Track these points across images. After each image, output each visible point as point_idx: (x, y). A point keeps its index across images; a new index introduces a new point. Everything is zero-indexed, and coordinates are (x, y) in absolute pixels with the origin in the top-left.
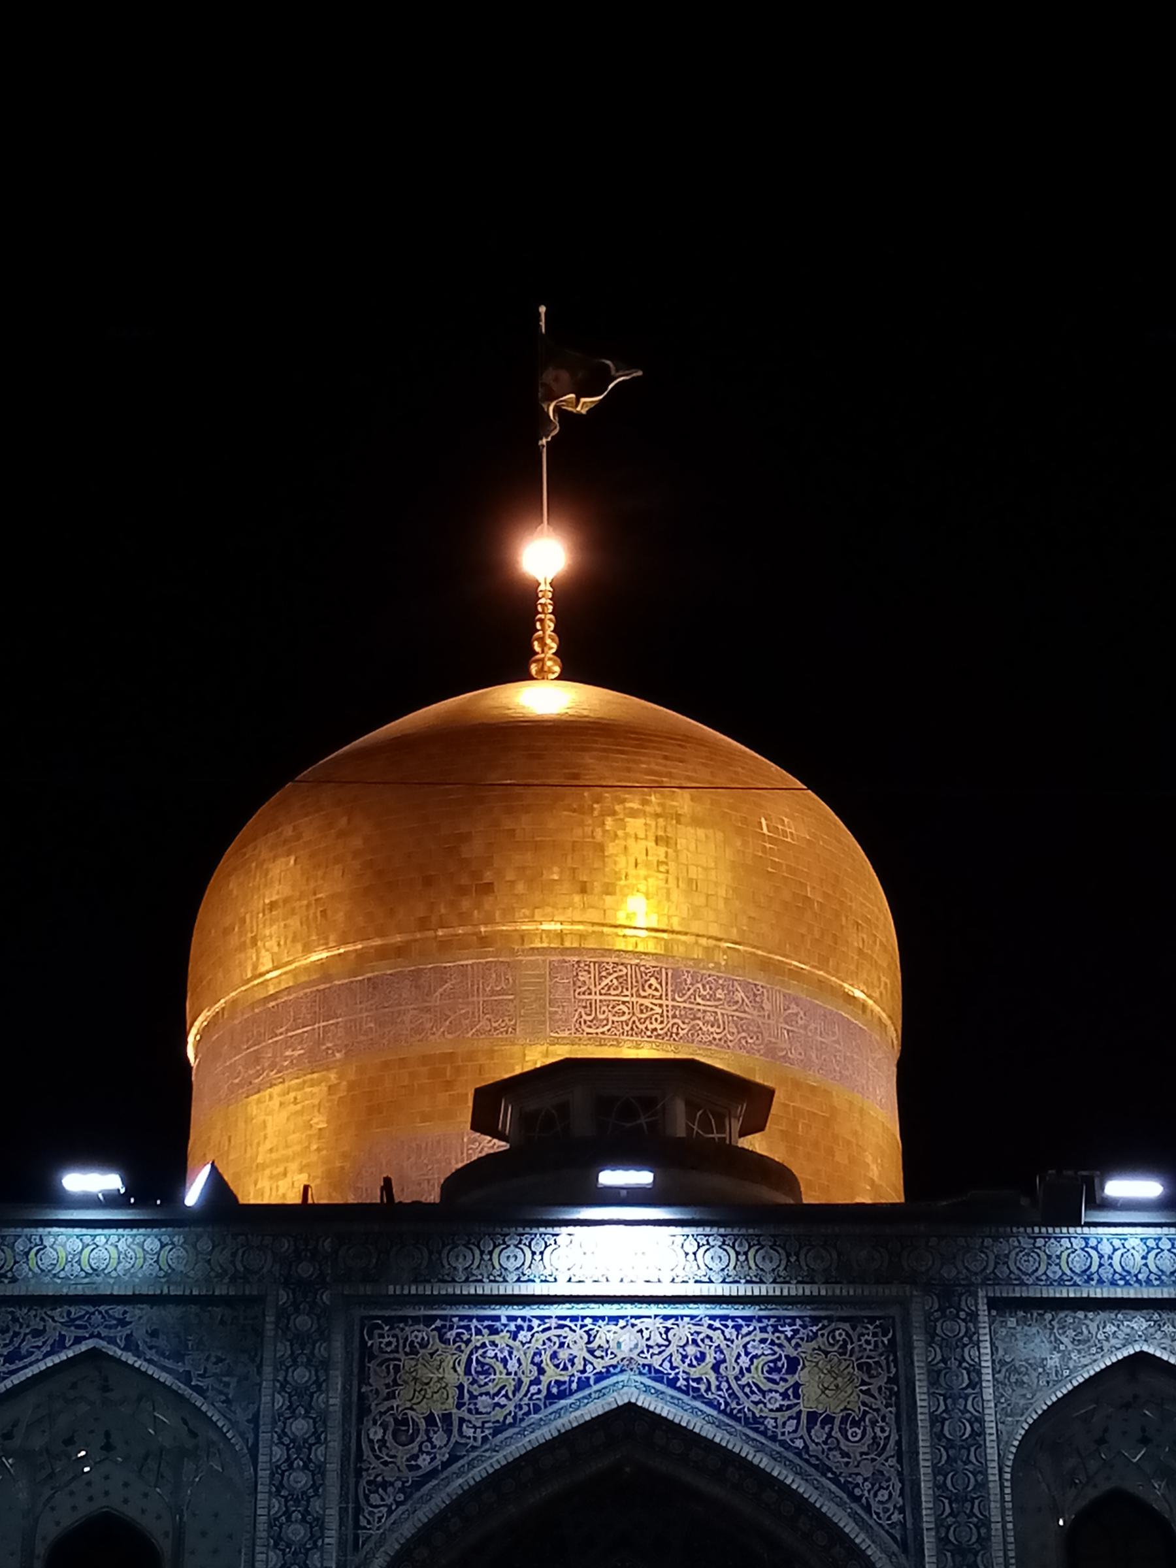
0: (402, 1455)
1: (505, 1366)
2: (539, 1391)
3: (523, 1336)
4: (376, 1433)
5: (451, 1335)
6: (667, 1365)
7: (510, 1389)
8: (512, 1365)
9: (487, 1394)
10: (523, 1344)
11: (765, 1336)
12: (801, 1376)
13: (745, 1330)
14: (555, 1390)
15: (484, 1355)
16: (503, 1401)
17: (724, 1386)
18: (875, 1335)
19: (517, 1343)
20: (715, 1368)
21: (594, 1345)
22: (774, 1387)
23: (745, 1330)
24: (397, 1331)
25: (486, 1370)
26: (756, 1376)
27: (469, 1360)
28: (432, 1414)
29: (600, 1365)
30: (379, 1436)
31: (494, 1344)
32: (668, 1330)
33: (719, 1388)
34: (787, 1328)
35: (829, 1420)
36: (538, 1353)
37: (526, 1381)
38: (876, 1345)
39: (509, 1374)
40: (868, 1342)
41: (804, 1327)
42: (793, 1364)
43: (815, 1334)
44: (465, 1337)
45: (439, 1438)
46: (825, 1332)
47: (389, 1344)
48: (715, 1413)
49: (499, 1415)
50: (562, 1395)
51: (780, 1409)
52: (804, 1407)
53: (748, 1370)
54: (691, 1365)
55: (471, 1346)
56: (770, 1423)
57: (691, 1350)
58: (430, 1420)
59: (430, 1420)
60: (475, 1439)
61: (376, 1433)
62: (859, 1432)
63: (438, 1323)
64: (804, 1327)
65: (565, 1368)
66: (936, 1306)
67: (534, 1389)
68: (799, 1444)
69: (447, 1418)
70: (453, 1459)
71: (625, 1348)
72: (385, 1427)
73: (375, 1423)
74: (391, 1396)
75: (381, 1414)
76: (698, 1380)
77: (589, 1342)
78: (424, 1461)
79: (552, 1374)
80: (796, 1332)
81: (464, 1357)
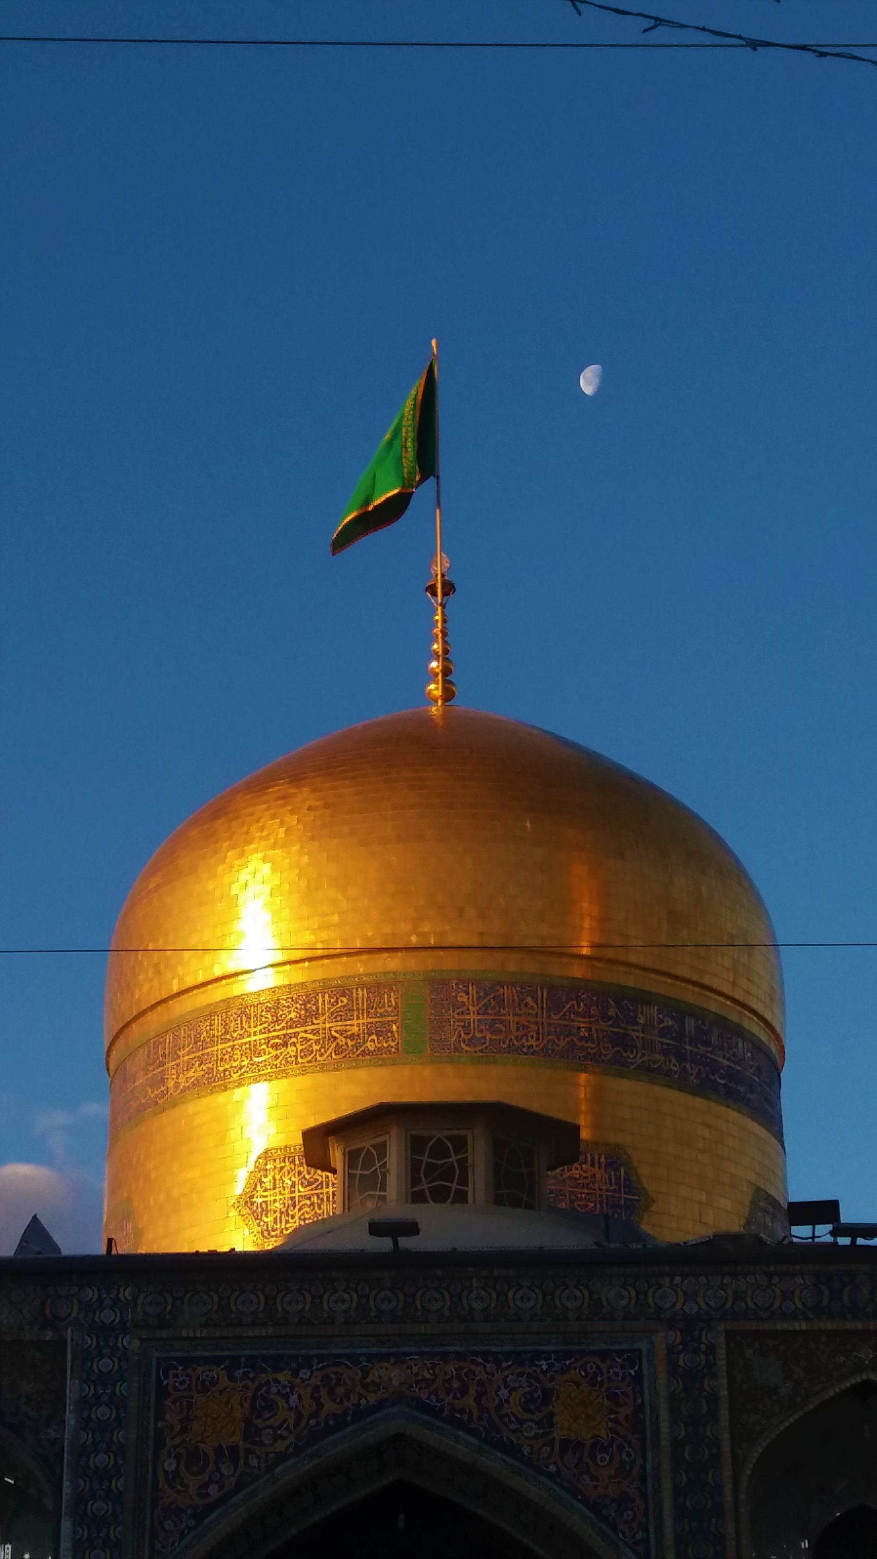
1: (287, 1402)
2: (318, 1424)
3: (304, 1373)
4: (170, 1465)
5: (238, 1373)
6: (434, 1398)
7: (291, 1422)
8: (294, 1399)
9: (271, 1427)
10: (303, 1380)
11: (520, 1370)
13: (504, 1365)
14: (331, 1423)
15: (268, 1391)
16: (285, 1433)
17: (485, 1415)
18: (622, 1368)
19: (298, 1380)
20: (477, 1400)
21: (368, 1380)
22: (530, 1416)
23: (504, 1365)
24: (190, 1371)
27: (254, 1397)
28: (220, 1446)
29: (372, 1399)
30: (173, 1467)
31: (277, 1381)
32: (434, 1366)
33: (480, 1418)
34: (543, 1362)
35: (580, 1445)
36: (316, 1389)
37: (306, 1413)
38: (623, 1378)
39: (290, 1409)
40: (616, 1374)
41: (558, 1360)
42: (547, 1396)
43: (569, 1367)
44: (251, 1375)
45: (226, 1469)
46: (578, 1365)
47: (182, 1383)
48: (476, 1441)
49: (281, 1446)
51: (536, 1437)
52: (557, 1435)
53: (507, 1401)
54: (455, 1398)
55: (257, 1383)
56: (526, 1450)
57: (456, 1384)
59: (219, 1451)
60: (259, 1468)
61: (170, 1465)
62: (607, 1457)
63: (227, 1363)
64: (558, 1360)
65: (341, 1403)
66: (679, 1340)
67: (312, 1422)
68: (552, 1468)
69: (234, 1450)
71: (395, 1383)
72: (178, 1458)
73: (169, 1454)
74: (184, 1430)
75: (175, 1447)
76: (462, 1411)
77: (364, 1377)
79: (329, 1407)
80: (550, 1366)
81: (250, 1394)
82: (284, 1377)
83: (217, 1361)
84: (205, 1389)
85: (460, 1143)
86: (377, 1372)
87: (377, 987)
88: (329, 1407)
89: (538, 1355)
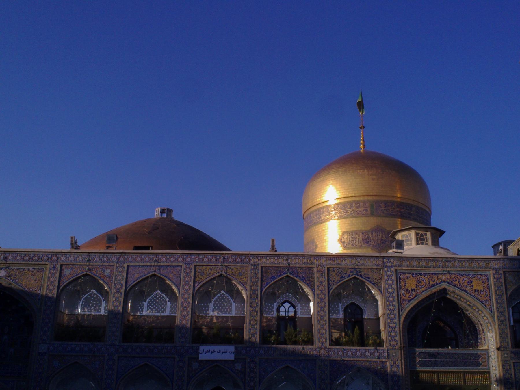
0: (408, 295)
3: (426, 276)
4: (403, 292)
8: (425, 281)
12: (473, 283)
25: (420, 282)
26: (466, 283)
35: (478, 291)
42: (471, 282)
45: (413, 293)
50: (433, 286)
52: (474, 289)
58: (412, 290)
59: (412, 290)
61: (403, 292)
69: (414, 289)
70: (416, 296)
78: (411, 296)
79: (431, 283)
82: (423, 277)
83: (410, 273)
84: (408, 278)
85: (426, 234)
86: (440, 276)
87: (364, 202)
88: (431, 283)
89: (469, 274)
